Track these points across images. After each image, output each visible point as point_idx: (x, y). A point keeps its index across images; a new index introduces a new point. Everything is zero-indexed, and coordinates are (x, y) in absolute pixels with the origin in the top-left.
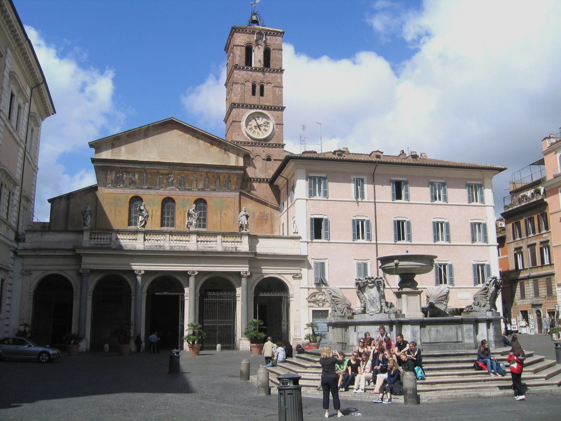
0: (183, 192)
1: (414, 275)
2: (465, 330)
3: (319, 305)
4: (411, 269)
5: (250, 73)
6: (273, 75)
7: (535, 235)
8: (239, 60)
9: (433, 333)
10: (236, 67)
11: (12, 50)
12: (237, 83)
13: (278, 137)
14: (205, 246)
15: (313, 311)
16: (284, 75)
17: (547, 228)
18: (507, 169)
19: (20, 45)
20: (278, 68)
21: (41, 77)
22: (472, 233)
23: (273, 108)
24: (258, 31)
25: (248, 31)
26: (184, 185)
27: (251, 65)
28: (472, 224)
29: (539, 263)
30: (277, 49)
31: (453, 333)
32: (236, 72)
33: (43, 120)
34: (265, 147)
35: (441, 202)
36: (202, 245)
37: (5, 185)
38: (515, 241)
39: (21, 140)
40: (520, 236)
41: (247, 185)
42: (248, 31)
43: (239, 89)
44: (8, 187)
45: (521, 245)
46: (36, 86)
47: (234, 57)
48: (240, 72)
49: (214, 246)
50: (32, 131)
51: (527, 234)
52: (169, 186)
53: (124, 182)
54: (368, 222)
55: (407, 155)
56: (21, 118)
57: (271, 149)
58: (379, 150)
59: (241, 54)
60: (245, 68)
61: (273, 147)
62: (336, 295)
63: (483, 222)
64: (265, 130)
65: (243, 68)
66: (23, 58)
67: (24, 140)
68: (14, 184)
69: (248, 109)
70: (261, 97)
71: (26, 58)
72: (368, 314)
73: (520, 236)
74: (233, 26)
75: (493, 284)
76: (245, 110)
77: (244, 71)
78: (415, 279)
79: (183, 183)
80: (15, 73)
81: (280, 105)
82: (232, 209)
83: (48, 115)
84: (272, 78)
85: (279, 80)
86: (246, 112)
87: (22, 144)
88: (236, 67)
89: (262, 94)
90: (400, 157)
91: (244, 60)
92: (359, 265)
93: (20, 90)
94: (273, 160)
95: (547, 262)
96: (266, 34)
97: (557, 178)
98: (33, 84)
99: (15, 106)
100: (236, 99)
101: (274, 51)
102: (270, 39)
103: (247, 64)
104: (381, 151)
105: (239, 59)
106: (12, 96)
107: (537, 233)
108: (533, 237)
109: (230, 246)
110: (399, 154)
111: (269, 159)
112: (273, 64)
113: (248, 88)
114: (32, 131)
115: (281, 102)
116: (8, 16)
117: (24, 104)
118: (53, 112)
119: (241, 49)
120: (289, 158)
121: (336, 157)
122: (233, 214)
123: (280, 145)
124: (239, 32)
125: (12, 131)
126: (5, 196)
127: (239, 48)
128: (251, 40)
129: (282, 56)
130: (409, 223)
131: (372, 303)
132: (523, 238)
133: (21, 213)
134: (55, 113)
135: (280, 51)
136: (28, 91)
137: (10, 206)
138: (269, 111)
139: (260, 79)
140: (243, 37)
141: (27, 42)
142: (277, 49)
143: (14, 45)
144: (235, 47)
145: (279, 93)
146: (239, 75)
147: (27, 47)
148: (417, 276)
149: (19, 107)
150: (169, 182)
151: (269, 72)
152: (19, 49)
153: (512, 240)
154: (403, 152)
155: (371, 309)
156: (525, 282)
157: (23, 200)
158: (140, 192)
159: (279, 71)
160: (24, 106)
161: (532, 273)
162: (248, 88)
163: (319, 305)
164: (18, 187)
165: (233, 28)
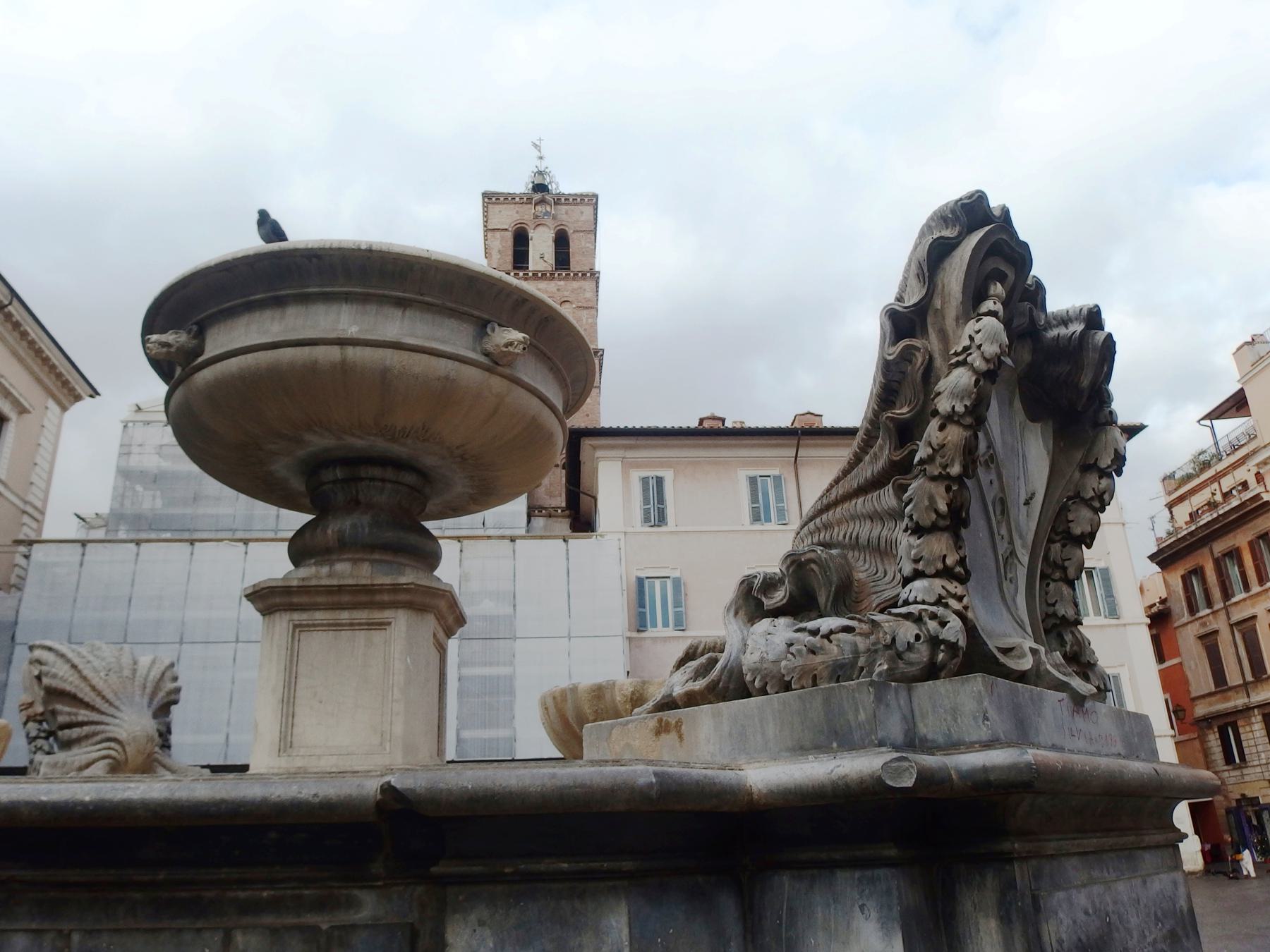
6: (575, 284)
7: (1252, 593)
8: (499, 259)
13: (588, 415)
18: (1146, 426)
20: (586, 268)
30: (582, 231)
33: (64, 409)
38: (1197, 619)
40: (1209, 604)
45: (1214, 626)
51: (1227, 594)
58: (812, 412)
59: (503, 247)
73: (1209, 604)
74: (483, 191)
83: (78, 398)
84: (573, 291)
85: (589, 295)
102: (567, 213)
104: (816, 413)
105: (499, 257)
107: (1256, 589)
108: (1244, 600)
112: (576, 263)
119: (502, 238)
124: (498, 202)
127: (498, 234)
128: (526, 217)
132: (1216, 607)
134: (98, 394)
142: (582, 231)
145: (590, 321)
151: (563, 279)
153: (1186, 618)
156: (1240, 723)
159: (588, 275)
161: (1258, 694)
165: (483, 194)
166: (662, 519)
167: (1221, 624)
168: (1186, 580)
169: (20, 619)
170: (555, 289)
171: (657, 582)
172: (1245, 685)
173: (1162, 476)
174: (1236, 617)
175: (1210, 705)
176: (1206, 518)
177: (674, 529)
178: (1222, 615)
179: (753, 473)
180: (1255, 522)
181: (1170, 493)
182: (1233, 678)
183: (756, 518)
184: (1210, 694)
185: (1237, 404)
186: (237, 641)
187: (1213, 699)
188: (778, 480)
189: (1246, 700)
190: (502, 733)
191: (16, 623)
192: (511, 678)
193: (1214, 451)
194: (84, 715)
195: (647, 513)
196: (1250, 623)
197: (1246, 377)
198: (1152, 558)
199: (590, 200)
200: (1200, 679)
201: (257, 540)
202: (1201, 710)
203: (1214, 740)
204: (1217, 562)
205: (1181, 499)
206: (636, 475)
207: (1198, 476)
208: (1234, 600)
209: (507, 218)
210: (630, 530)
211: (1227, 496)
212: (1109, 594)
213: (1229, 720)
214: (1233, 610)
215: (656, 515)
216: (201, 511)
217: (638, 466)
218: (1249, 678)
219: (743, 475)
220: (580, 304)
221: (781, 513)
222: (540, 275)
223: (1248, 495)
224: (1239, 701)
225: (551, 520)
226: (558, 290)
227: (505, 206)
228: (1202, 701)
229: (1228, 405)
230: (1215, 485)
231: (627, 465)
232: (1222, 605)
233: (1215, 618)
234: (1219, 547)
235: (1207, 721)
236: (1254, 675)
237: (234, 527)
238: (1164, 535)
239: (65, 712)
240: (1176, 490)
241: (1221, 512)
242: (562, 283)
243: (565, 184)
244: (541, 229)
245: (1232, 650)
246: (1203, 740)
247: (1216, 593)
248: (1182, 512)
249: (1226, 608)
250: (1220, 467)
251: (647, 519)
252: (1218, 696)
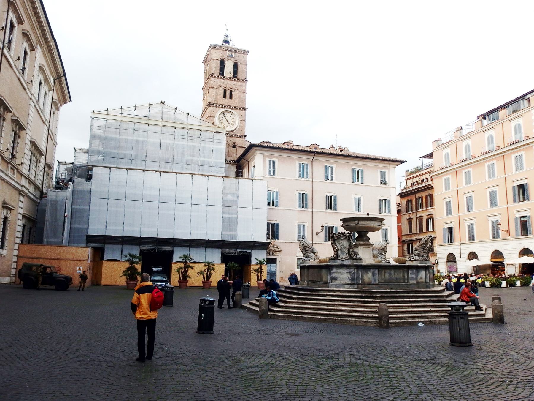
1: (367, 232)
2: (409, 274)
3: (269, 254)
4: (365, 227)
5: (222, 81)
6: (240, 83)
9: (387, 276)
10: (212, 75)
11: (41, 46)
12: (213, 88)
13: (241, 130)
16: (248, 83)
17: (432, 205)
19: (47, 42)
21: (62, 71)
22: (380, 207)
23: (239, 108)
24: (229, 49)
25: (222, 49)
27: (223, 75)
28: (380, 200)
29: (424, 230)
30: (243, 64)
31: (401, 275)
32: (212, 79)
34: (232, 137)
35: (359, 183)
37: (34, 154)
39: (46, 120)
42: (222, 49)
43: (214, 92)
44: (37, 156)
45: (412, 217)
46: (58, 78)
47: (211, 67)
48: (215, 79)
50: (54, 113)
51: (417, 209)
54: (306, 195)
55: (335, 149)
56: (47, 102)
57: (236, 139)
59: (216, 66)
60: (219, 77)
61: (237, 138)
62: (307, 245)
63: (388, 199)
64: (232, 124)
65: (218, 77)
66: (49, 54)
67: (48, 120)
68: (40, 155)
69: (220, 108)
70: (230, 100)
71: (51, 54)
72: (340, 259)
73: (412, 210)
75: (430, 241)
76: (218, 108)
77: (218, 79)
78: (368, 235)
80: (43, 65)
81: (244, 107)
83: (65, 102)
85: (244, 88)
86: (219, 110)
87: (46, 123)
88: (212, 75)
89: (231, 97)
90: (330, 149)
91: (218, 71)
92: (299, 226)
93: (46, 80)
94: (237, 147)
95: (430, 229)
96: (236, 52)
97: (442, 170)
98: (56, 77)
99: (43, 93)
100: (210, 100)
101: (241, 65)
102: (238, 56)
103: (220, 74)
106: (41, 83)
107: (425, 209)
110: (330, 147)
111: (234, 146)
112: (240, 75)
113: (221, 92)
114: (54, 113)
115: (245, 104)
116: (40, 18)
117: (49, 91)
118: (69, 100)
120: (251, 146)
121: (285, 146)
123: (243, 136)
125: (40, 112)
126: (34, 163)
127: (215, 61)
129: (246, 70)
130: (336, 197)
131: (342, 252)
132: (414, 212)
133: (45, 177)
134: (71, 101)
135: (245, 66)
136: (52, 81)
137: (37, 171)
138: (236, 111)
139: (230, 86)
140: (219, 53)
141: (53, 41)
142: (243, 64)
143: (43, 42)
144: (212, 60)
145: (244, 97)
147: (53, 45)
148: (369, 233)
149: (46, 94)
152: (46, 47)
153: (405, 213)
154: (333, 146)
155: (341, 256)
156: (413, 243)
157: (46, 167)
159: (244, 81)
160: (49, 93)
162: (221, 92)
163: (269, 254)
164: (43, 157)
165: (211, 45)
166: (274, 174)
167: (414, 216)
168: (407, 202)
169: (92, 190)
170: (233, 84)
171: (271, 192)
172: (417, 234)
173: (406, 170)
174: (418, 215)
175: (407, 237)
176: (416, 187)
177: (277, 177)
178: (415, 214)
179: (300, 162)
180: (427, 191)
181: (407, 176)
182: (414, 231)
183: (300, 176)
184: (407, 235)
185: (431, 156)
186: (159, 202)
187: (408, 236)
188: (307, 165)
189: (416, 238)
190: (234, 233)
191: (91, 191)
192: (237, 218)
193: (421, 167)
194: (309, 249)
195: (270, 171)
196: (421, 218)
197: (435, 150)
198: (399, 194)
199: (246, 52)
200: (406, 231)
201: (163, 172)
202: (404, 239)
203: (406, 247)
204: (417, 200)
205: (410, 179)
206: (267, 160)
207: (416, 173)
208: (418, 211)
209: (217, 55)
210: (265, 176)
211: (422, 181)
212: (389, 207)
213: (411, 242)
214: (418, 213)
215: (272, 172)
216: (120, 152)
217: (268, 157)
218: (418, 232)
219: (297, 163)
220: (241, 91)
221: (307, 175)
222: (228, 78)
223: (428, 183)
224: (414, 238)
225: (231, 165)
226: (234, 85)
227: (217, 50)
228: (405, 236)
229: (428, 155)
230: (420, 177)
231: (265, 156)
232: (415, 211)
233: (413, 215)
234: (418, 195)
235: (404, 242)
236: (419, 232)
237: (132, 158)
238: (403, 188)
239: (307, 249)
240: (409, 175)
241: (420, 186)
242: (235, 82)
243: (236, 43)
244: (229, 61)
245: (415, 224)
246: (403, 247)
247: (414, 208)
248: (410, 182)
249: (416, 212)
250: (422, 172)
251: (269, 174)
252: (409, 235)
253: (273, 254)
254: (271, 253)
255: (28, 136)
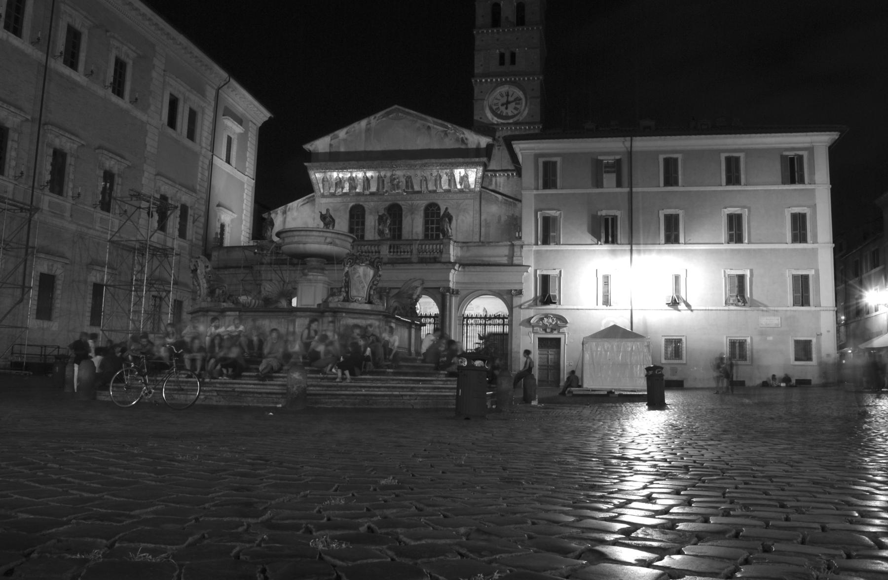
0: (410, 196)
3: (546, 332)
14: (398, 257)
15: (539, 338)
26: (412, 187)
36: (394, 257)
41: (491, 180)
49: (409, 256)
52: (395, 190)
53: (343, 188)
79: (410, 184)
82: (471, 213)
89: (513, 62)
109: (428, 256)
122: (472, 219)
146: (482, 41)
150: (393, 185)
158: (362, 201)
226: (517, 39)
253: (552, 330)
254: (548, 330)
255: (146, 174)
